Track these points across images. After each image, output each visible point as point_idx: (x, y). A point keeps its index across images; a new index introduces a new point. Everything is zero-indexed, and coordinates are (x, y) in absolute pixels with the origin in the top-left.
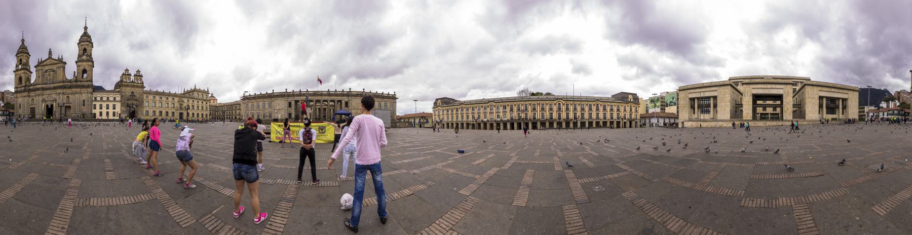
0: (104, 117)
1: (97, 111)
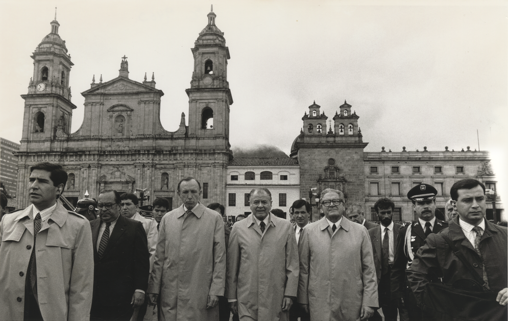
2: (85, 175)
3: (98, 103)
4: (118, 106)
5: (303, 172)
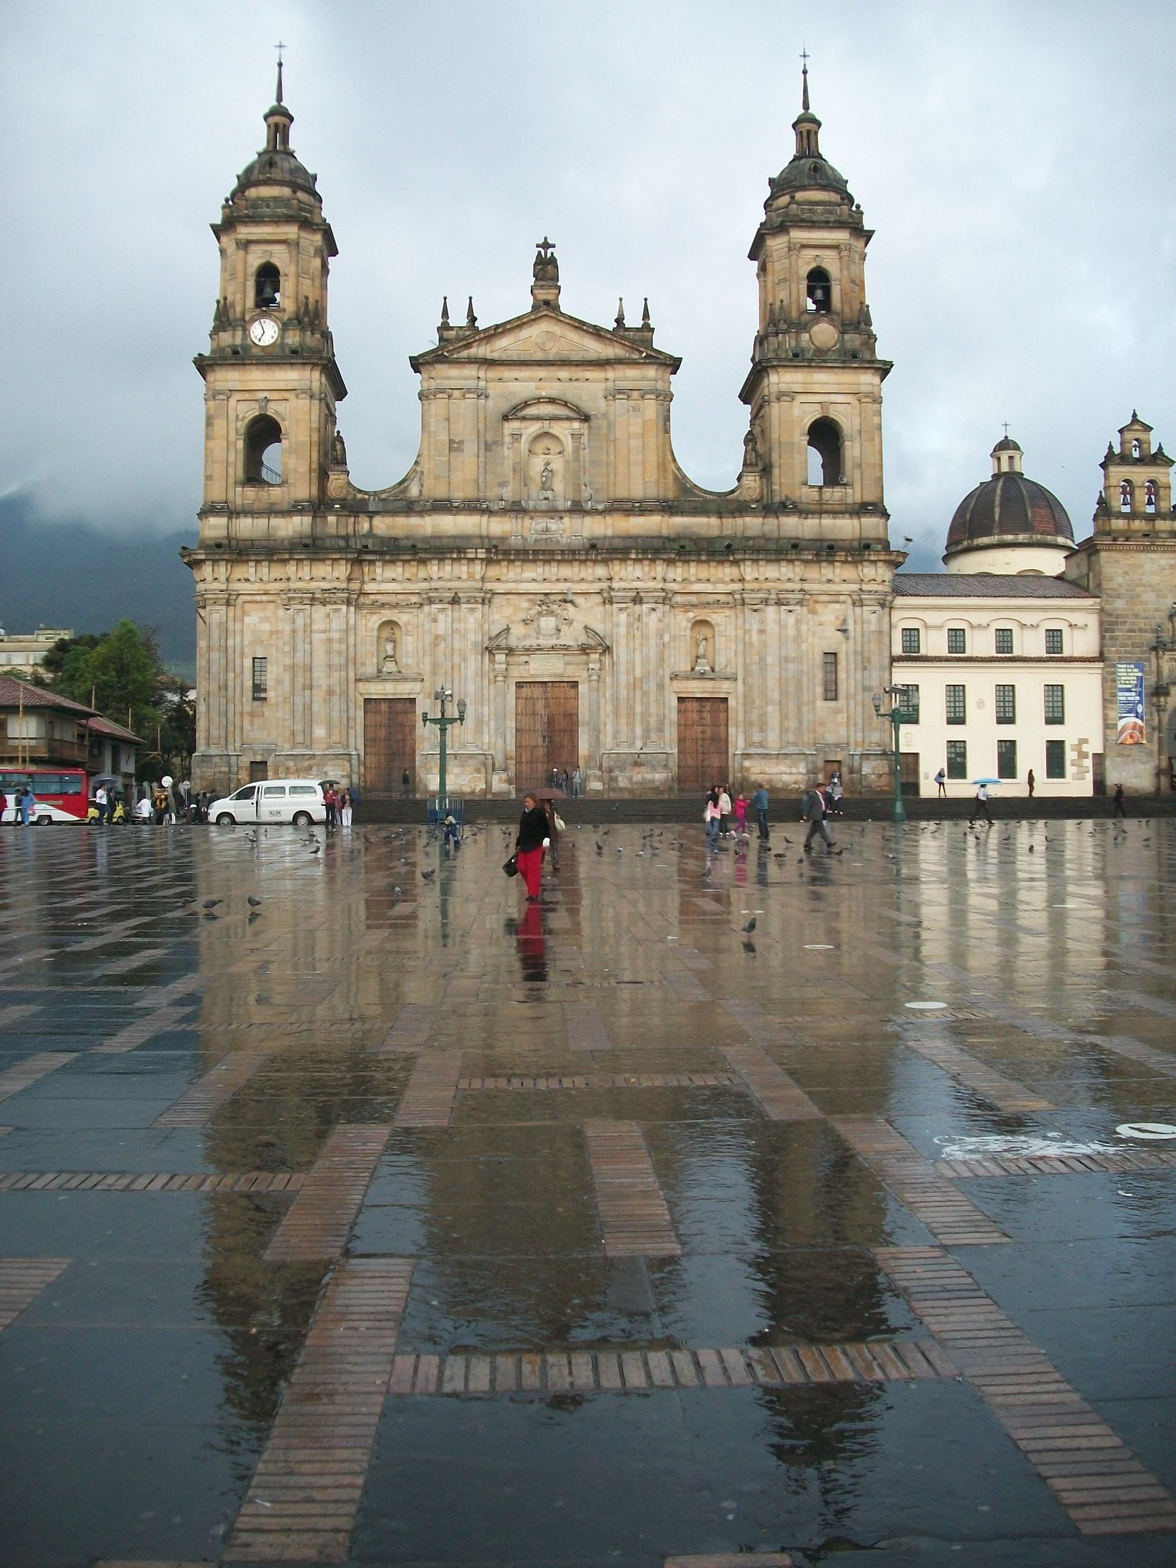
0: (981, 777)
1: (926, 741)
2: (442, 627)
3: (469, 390)
4: (538, 400)
5: (1111, 623)
